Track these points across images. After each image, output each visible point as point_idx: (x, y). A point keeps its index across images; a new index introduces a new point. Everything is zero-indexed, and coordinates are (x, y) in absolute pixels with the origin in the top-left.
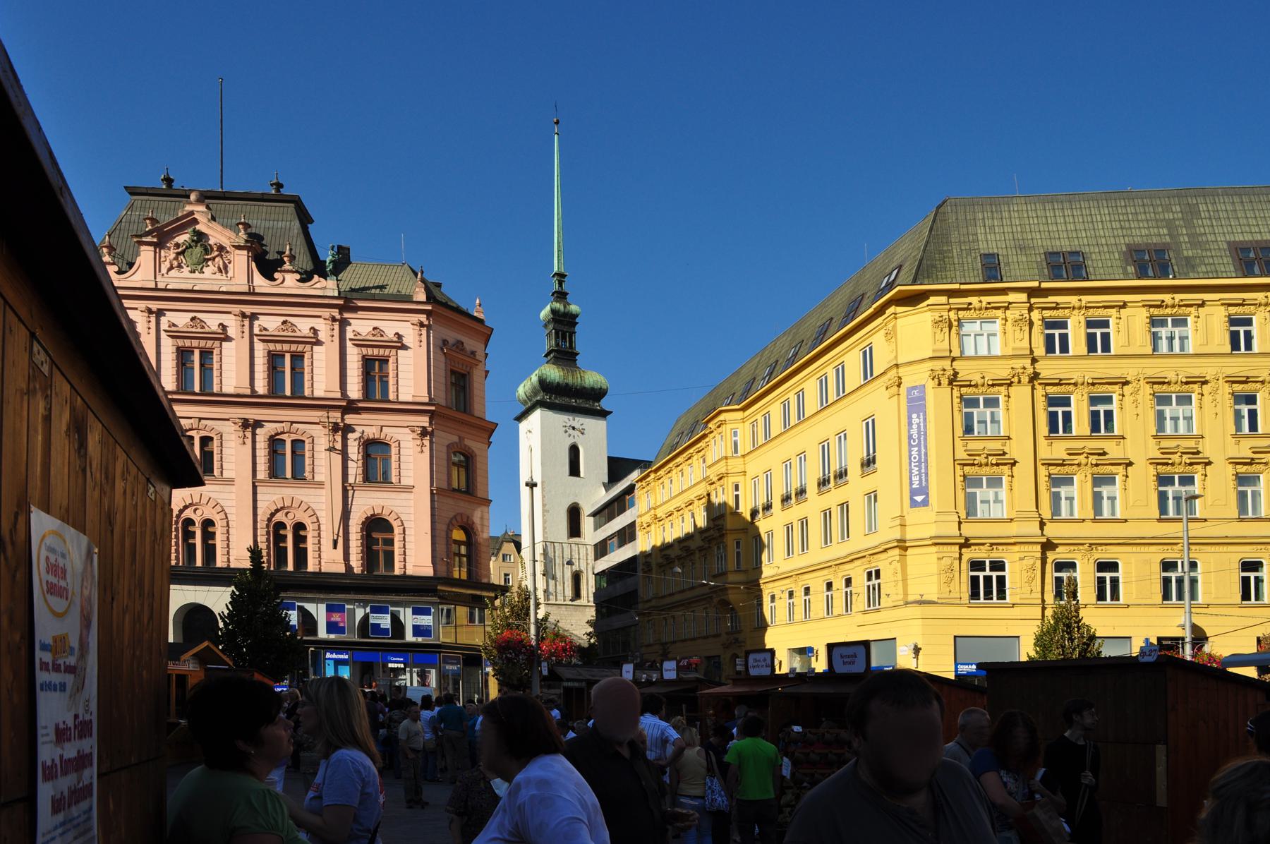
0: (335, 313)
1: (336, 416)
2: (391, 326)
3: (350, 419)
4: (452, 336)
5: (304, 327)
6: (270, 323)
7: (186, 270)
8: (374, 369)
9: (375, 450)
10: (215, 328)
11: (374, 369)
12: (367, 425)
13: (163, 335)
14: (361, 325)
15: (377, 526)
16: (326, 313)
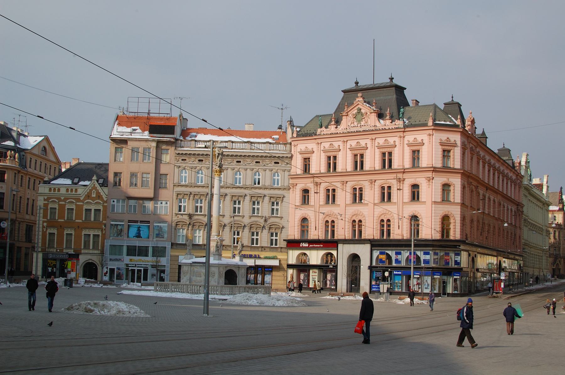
0: (401, 134)
1: (400, 176)
2: (421, 136)
3: (405, 176)
4: (443, 136)
5: (391, 140)
6: (381, 141)
7: (356, 124)
8: (416, 155)
9: (415, 187)
10: (364, 145)
11: (416, 155)
12: (410, 180)
13: (348, 150)
14: (410, 137)
15: (414, 218)
16: (398, 134)
